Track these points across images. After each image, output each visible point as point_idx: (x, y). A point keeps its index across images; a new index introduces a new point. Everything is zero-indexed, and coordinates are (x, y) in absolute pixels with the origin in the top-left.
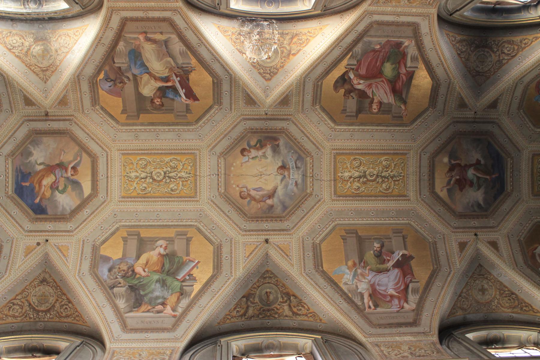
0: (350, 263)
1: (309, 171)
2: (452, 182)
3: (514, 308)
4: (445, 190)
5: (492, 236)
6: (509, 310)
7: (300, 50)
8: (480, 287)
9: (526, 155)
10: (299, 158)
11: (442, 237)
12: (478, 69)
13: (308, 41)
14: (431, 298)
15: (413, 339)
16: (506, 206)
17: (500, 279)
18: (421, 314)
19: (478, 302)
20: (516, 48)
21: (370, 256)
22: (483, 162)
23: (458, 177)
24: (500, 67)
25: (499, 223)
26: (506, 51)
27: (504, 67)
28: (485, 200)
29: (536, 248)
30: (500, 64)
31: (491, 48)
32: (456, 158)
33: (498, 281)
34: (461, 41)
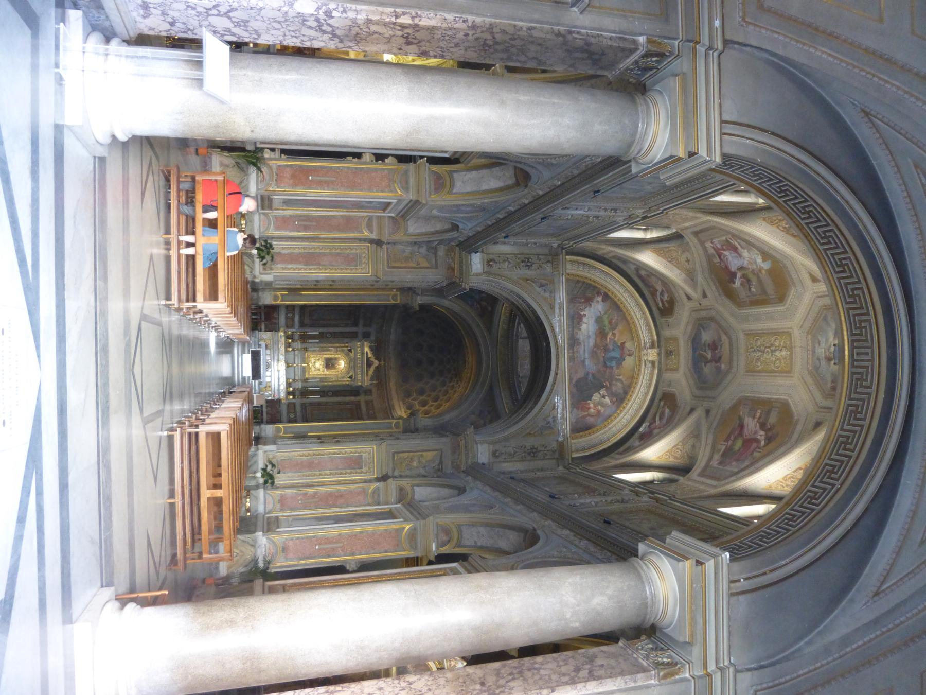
0: (764, 272)
1: (810, 356)
7: (795, 471)
10: (817, 368)
13: (785, 478)
14: (701, 252)
16: (690, 328)
21: (754, 281)
30: (684, 442)
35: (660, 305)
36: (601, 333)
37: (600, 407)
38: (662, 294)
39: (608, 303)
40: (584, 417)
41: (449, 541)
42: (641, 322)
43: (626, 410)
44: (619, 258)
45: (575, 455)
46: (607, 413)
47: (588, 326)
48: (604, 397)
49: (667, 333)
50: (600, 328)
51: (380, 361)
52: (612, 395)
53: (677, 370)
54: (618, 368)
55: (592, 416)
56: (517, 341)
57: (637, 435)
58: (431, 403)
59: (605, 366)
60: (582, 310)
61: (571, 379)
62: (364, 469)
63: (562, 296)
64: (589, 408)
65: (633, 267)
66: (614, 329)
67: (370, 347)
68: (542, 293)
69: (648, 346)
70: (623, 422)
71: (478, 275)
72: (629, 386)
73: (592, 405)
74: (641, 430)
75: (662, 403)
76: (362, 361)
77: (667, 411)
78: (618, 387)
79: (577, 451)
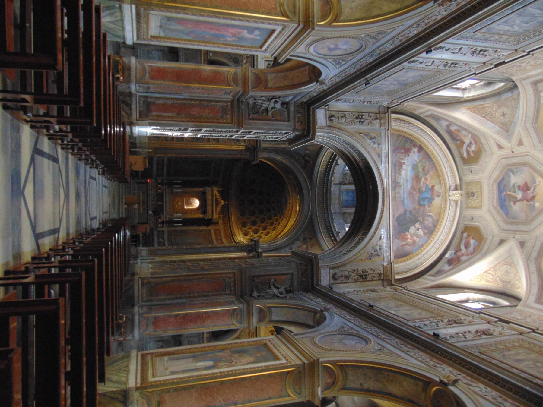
2: (532, 189)
3: (482, 108)
4: (538, 182)
5: (502, 152)
6: (485, 105)
8: (506, 116)
9: (485, 208)
11: (536, 148)
12: (510, 267)
15: (528, 74)
16: (496, 173)
17: (493, 125)
18: (534, 90)
19: (506, 106)
20: (484, 277)
22: (512, 203)
23: (529, 192)
24: (495, 266)
25: (499, 161)
26: (491, 276)
27: (493, 265)
28: (510, 177)
29: (475, 148)
31: (501, 280)
32: (530, 205)
33: (494, 123)
34: (519, 288)
35: (465, 155)
36: (417, 178)
37: (415, 238)
38: (469, 145)
39: (422, 154)
40: (403, 246)
41: (333, 383)
42: (448, 169)
43: (435, 240)
44: (433, 116)
45: (397, 277)
46: (420, 243)
47: (407, 173)
48: (418, 229)
49: (469, 178)
50: (415, 174)
51: (225, 201)
52: (425, 228)
53: (480, 207)
54: (429, 206)
55: (410, 245)
56: (331, 186)
57: (444, 260)
58: (261, 231)
59: (419, 204)
60: (402, 159)
61: (393, 216)
62: (228, 292)
63: (386, 147)
64: (407, 239)
65: (444, 123)
66: (427, 175)
67: (218, 191)
68: (372, 144)
69: (452, 188)
70: (433, 250)
71: (322, 128)
72: (437, 221)
73: (409, 236)
74: (447, 256)
75: (465, 235)
76: (212, 201)
77: (472, 241)
78: (429, 222)
79: (398, 273)
